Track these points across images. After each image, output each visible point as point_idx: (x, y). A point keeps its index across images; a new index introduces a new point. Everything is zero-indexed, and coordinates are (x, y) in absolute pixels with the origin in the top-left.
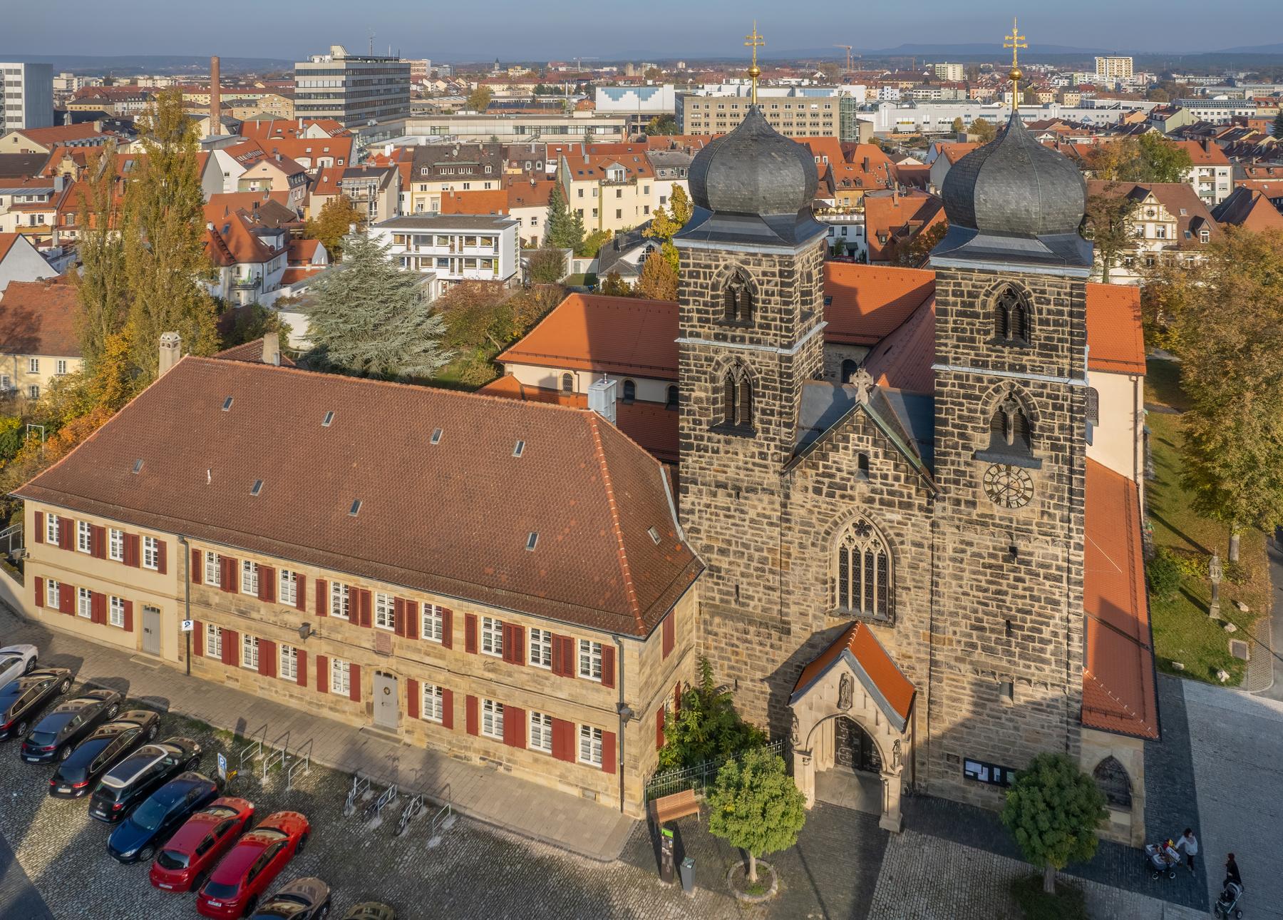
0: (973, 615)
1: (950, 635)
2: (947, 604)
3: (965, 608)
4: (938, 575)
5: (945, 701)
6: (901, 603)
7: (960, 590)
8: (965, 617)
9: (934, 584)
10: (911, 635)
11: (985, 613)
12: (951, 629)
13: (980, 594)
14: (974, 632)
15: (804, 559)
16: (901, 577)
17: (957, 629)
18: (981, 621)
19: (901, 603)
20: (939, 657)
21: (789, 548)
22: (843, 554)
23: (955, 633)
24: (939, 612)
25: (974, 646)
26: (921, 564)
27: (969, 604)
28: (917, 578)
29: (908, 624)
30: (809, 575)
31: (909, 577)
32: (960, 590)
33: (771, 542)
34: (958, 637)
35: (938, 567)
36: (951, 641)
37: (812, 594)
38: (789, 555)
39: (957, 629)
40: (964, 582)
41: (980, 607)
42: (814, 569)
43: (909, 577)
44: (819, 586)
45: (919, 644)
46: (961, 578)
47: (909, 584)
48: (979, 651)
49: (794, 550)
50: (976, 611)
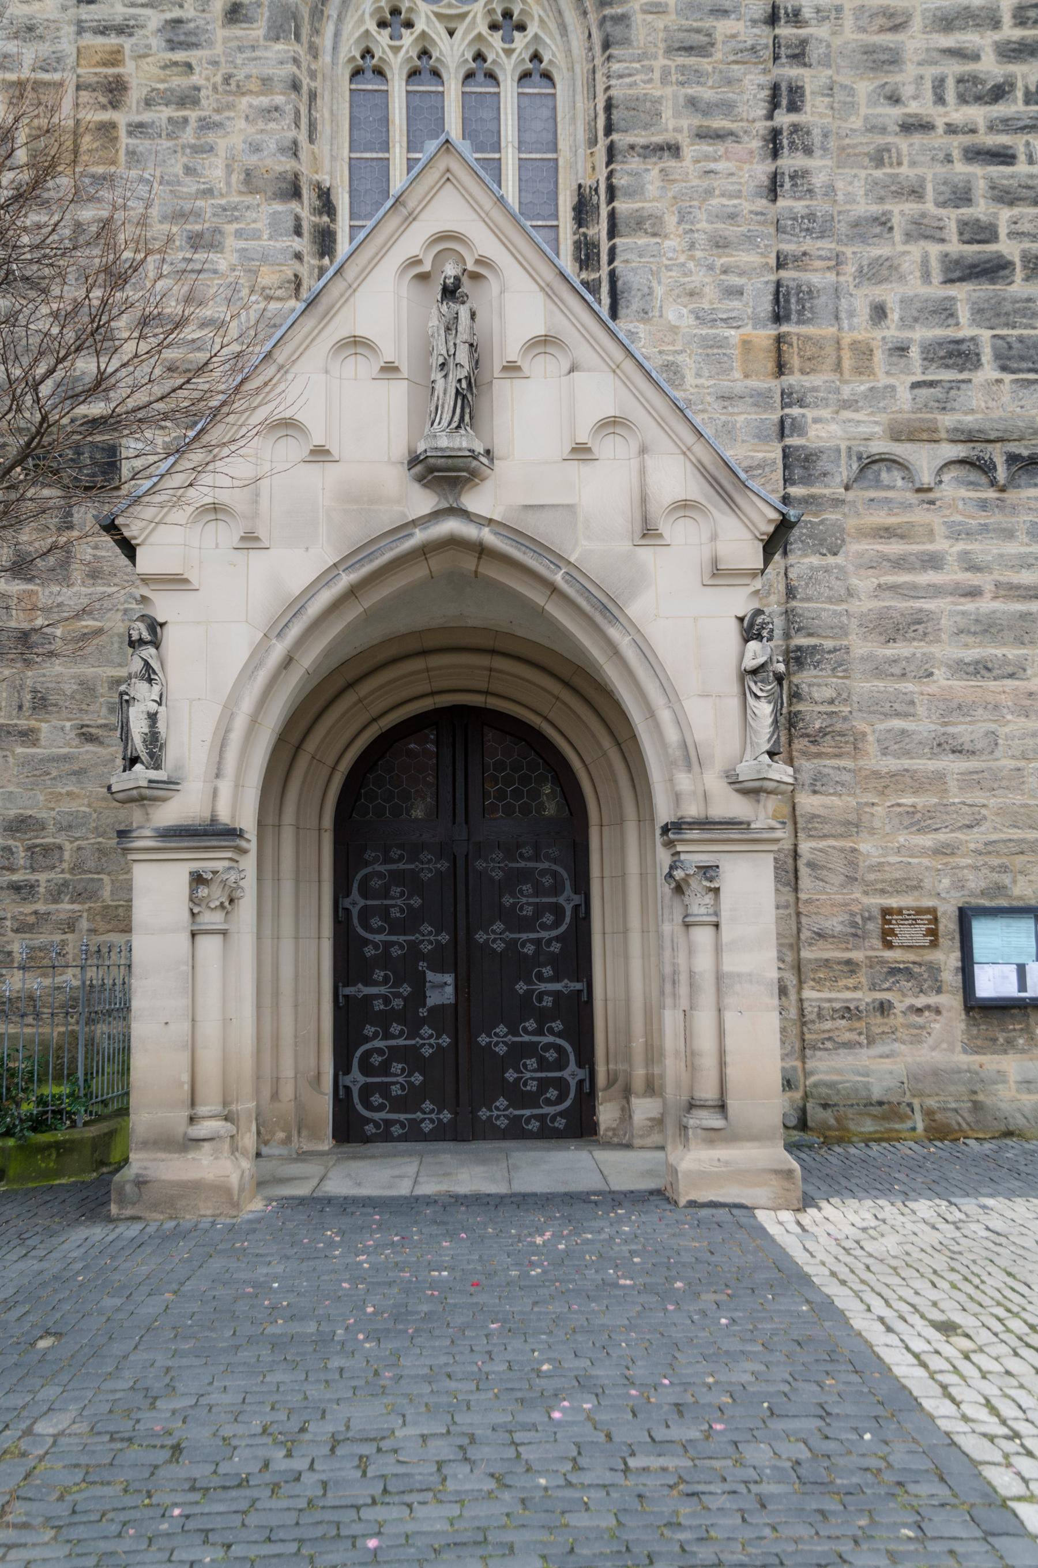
0: (951, 217)
1: (858, 328)
2: (844, 186)
3: (916, 193)
4: (799, 56)
5: (861, 646)
6: (639, 223)
7: (894, 113)
8: (923, 230)
9: (783, 97)
10: (688, 363)
11: (1005, 197)
12: (860, 301)
13: (977, 114)
14: (963, 293)
15: (188, 99)
16: (634, 104)
17: (890, 294)
18: (981, 232)
19: (639, 223)
20: (824, 431)
21: (114, 58)
22: (367, 68)
23: (879, 312)
24: (813, 225)
25: (960, 355)
26: (723, 27)
27: (931, 174)
28: (706, 94)
29: (676, 314)
30: (215, 171)
31: (669, 97)
32: (894, 113)
33: (29, 53)
34: (891, 331)
35: (796, 17)
36: (864, 352)
37: (222, 262)
38: (115, 91)
39: (890, 294)
40: (905, 78)
41: (981, 174)
42: (236, 136)
43: (669, 97)
44: (266, 212)
45: (726, 398)
46: (893, 60)
47: (675, 124)
48: (988, 371)
49: (140, 76)
50: (962, 197)
